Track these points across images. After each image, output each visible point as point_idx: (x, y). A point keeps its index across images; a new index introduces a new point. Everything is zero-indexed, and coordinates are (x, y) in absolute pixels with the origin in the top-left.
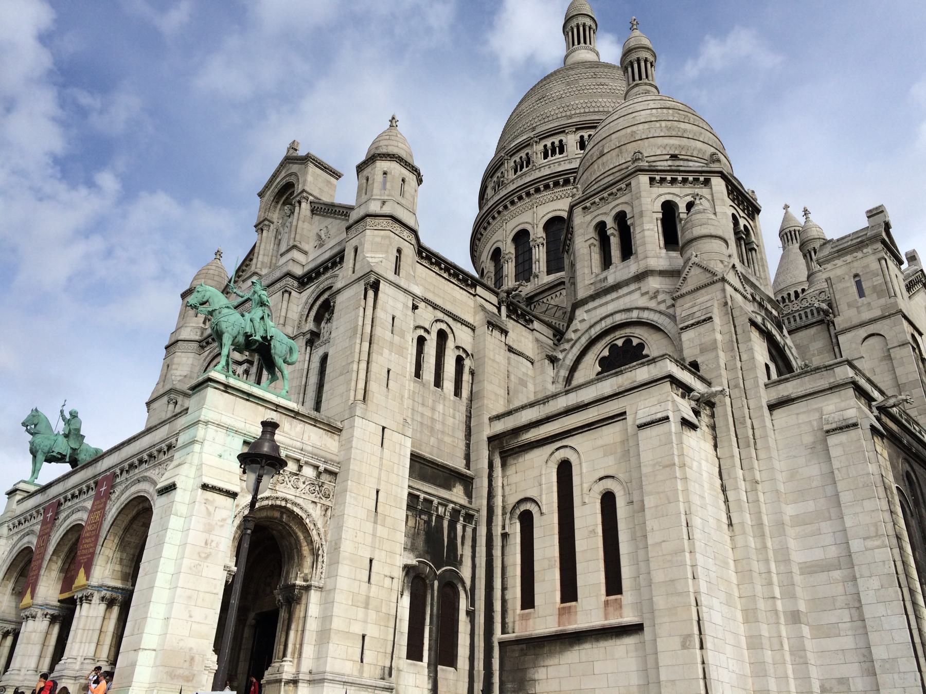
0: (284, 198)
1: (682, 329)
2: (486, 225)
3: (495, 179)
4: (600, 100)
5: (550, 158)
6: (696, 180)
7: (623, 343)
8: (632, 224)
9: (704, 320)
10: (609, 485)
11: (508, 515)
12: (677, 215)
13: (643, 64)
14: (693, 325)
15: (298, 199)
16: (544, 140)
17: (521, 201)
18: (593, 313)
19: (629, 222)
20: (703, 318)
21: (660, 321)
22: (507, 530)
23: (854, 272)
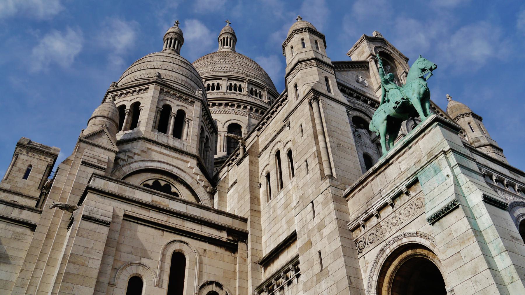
3: (233, 83)
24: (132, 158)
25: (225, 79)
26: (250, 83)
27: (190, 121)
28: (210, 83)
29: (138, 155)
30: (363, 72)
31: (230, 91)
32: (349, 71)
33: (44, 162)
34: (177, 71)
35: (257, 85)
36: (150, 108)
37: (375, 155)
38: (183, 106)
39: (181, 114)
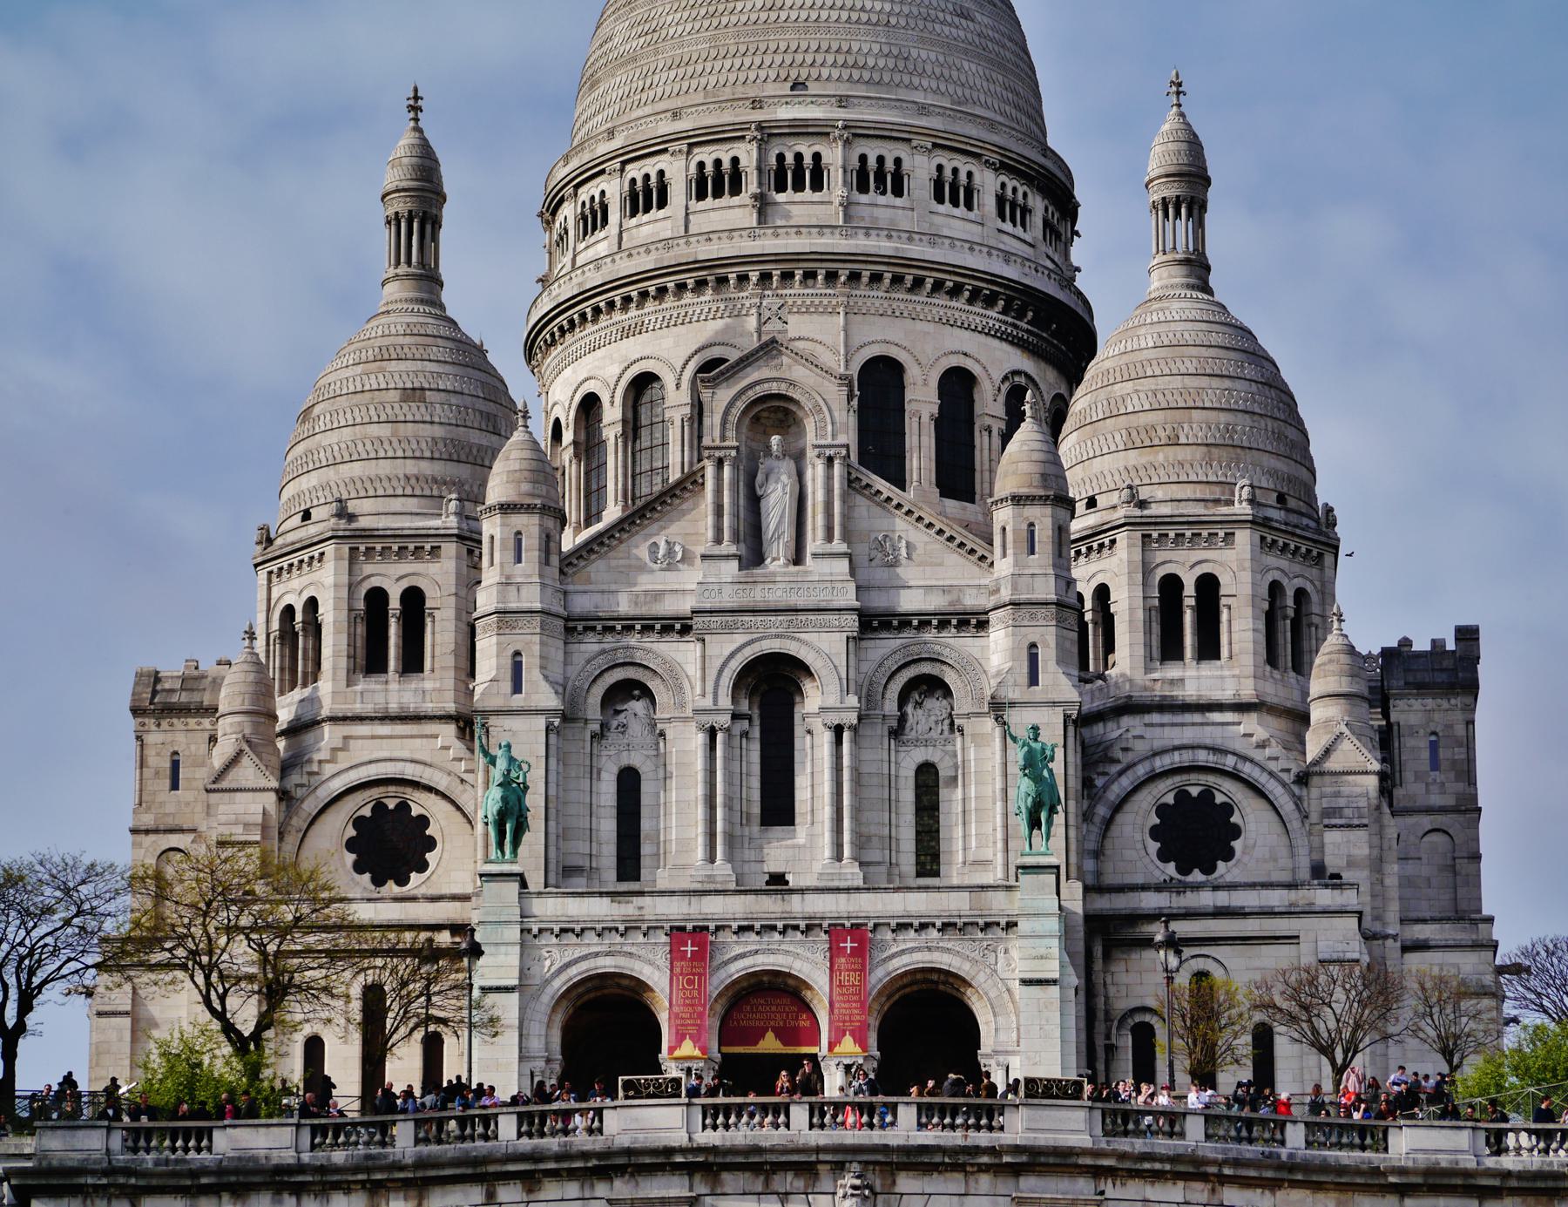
0: (756, 410)
1: (1326, 826)
2: (691, 283)
3: (707, 155)
4: (966, 64)
6: (1309, 551)
9: (1358, 826)
11: (1116, 1023)
12: (1278, 603)
13: (1196, 212)
15: (828, 452)
16: (863, 141)
17: (810, 282)
18: (1158, 730)
19: (1223, 601)
20: (1356, 822)
21: (1268, 786)
22: (1114, 1041)
24: (317, 774)
25: (677, 148)
26: (766, 134)
27: (436, 613)
28: (635, 171)
29: (328, 761)
30: (684, 506)
31: (702, 205)
32: (633, 536)
33: (199, 734)
34: (390, 454)
35: (800, 129)
36: (335, 622)
37: (648, 762)
38: (413, 574)
39: (414, 599)
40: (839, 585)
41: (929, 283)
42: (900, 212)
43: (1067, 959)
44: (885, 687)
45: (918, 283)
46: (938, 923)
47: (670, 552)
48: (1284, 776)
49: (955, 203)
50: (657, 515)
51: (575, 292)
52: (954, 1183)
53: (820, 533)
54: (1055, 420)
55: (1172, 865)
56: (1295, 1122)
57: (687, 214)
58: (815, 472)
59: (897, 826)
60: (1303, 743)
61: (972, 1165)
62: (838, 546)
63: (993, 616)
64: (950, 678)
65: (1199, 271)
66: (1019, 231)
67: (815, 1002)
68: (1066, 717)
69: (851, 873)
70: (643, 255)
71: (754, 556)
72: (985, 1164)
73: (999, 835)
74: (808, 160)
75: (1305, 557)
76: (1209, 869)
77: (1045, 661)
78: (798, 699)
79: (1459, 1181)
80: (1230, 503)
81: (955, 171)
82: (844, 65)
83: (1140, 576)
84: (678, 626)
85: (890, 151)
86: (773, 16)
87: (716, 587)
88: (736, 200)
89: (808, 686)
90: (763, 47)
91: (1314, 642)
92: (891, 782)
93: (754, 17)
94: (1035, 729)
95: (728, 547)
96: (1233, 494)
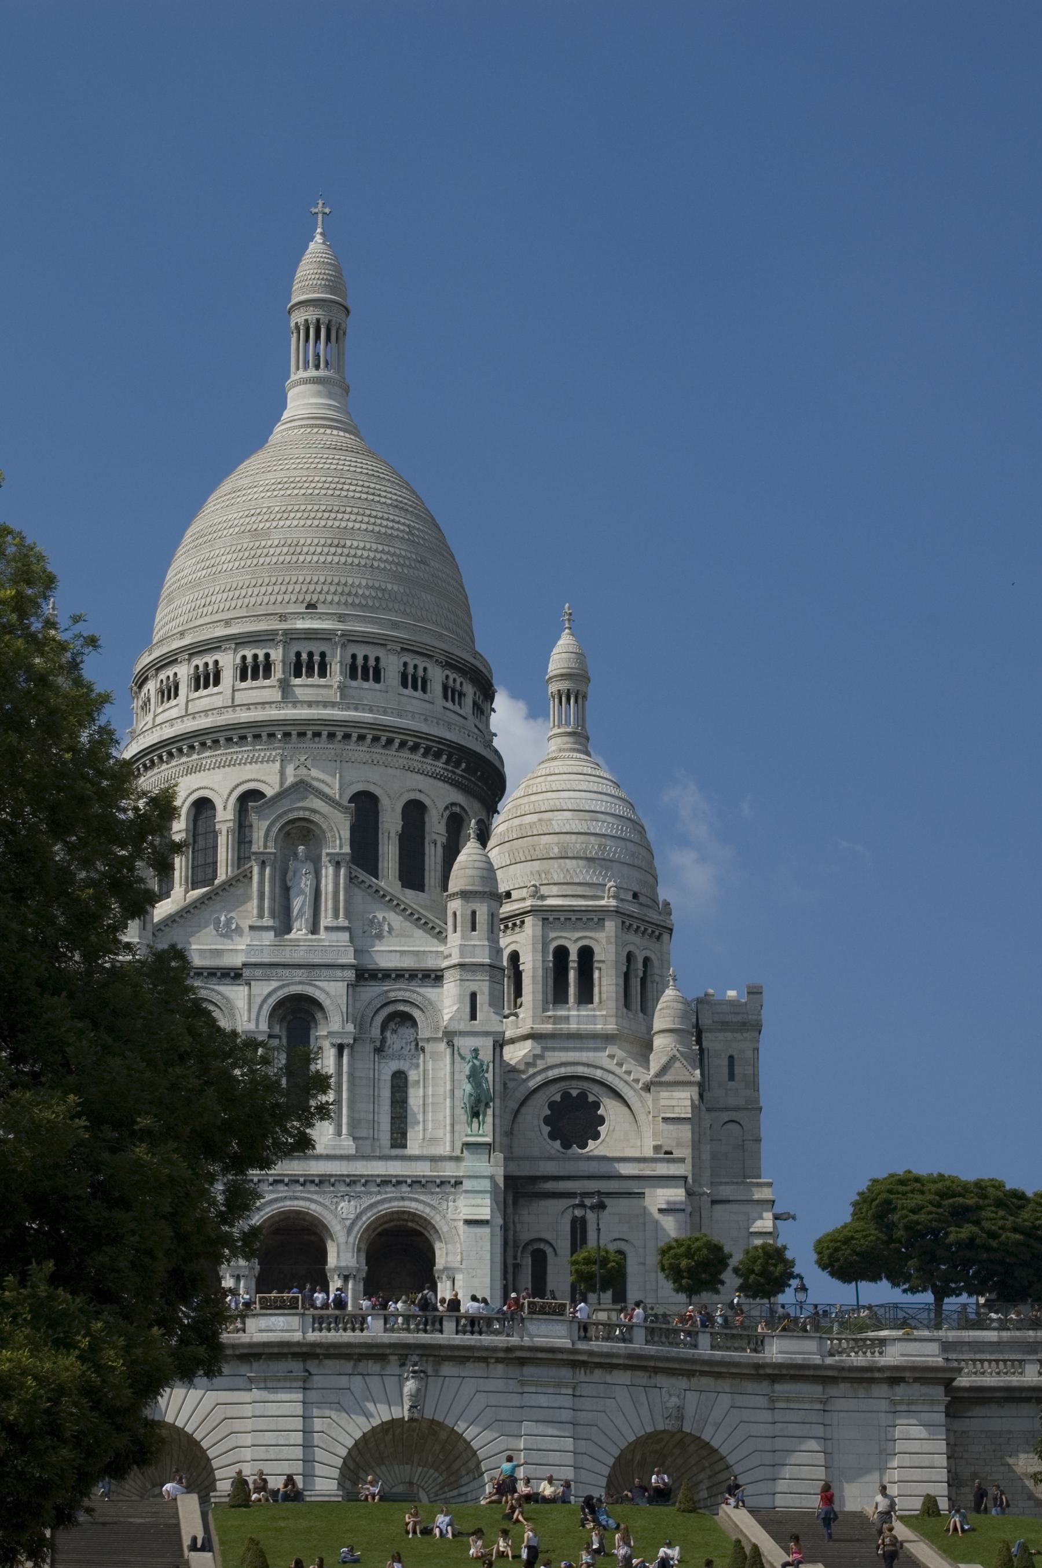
1: (663, 1118)
3: (249, 653)
5: (359, 683)
6: (653, 932)
7: (578, 1094)
8: (600, 969)
9: (684, 1118)
10: (622, 1246)
11: (520, 1249)
12: (632, 967)
13: (580, 700)
14: (673, 1118)
17: (317, 739)
19: (596, 965)
20: (683, 1116)
22: (519, 1261)
23: (730, 1052)
25: (228, 646)
26: (291, 637)
30: (238, 892)
31: (244, 685)
35: (310, 635)
40: (343, 948)
41: (397, 742)
42: (378, 693)
43: (496, 1207)
44: (372, 1019)
45: (390, 742)
46: (409, 1181)
47: (229, 922)
48: (634, 1084)
49: (415, 688)
50: (219, 898)
51: (156, 741)
52: (479, 1369)
53: (330, 913)
54: (483, 838)
55: (558, 1142)
56: (704, 1332)
57: (234, 691)
58: (328, 872)
59: (378, 1113)
60: (648, 1061)
61: (492, 1358)
62: (342, 922)
63: (447, 974)
64: (416, 1013)
65: (583, 740)
66: (457, 708)
67: (324, 1232)
68: (495, 1042)
69: (348, 1145)
70: (203, 717)
71: (285, 927)
72: (501, 1358)
73: (448, 1121)
74: (317, 658)
75: (650, 936)
76: (584, 1146)
77: (482, 1004)
78: (313, 1025)
79: (811, 1373)
80: (603, 898)
81: (415, 667)
82: (342, 594)
83: (540, 946)
84: (233, 975)
85: (372, 652)
86: (295, 558)
87: (259, 948)
88: (267, 682)
89: (319, 1016)
90: (287, 579)
91: (655, 993)
92: (375, 1084)
93: (281, 559)
94: (476, 1051)
95: (267, 921)
96: (604, 891)
